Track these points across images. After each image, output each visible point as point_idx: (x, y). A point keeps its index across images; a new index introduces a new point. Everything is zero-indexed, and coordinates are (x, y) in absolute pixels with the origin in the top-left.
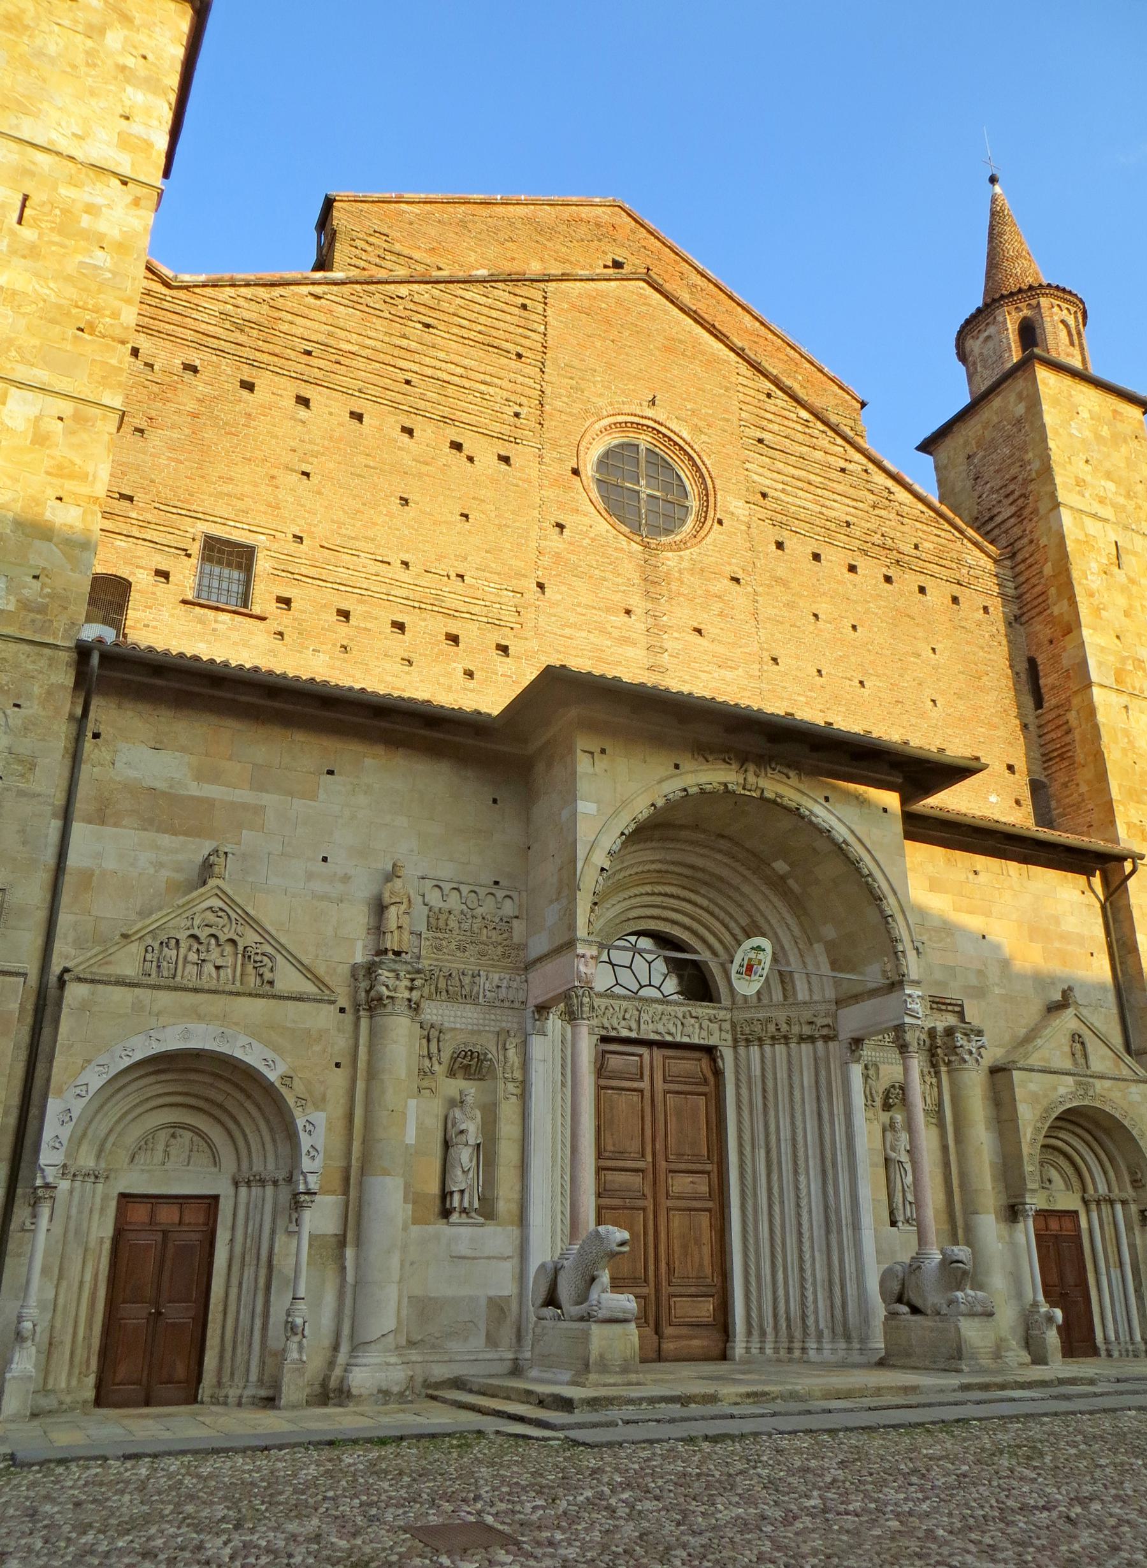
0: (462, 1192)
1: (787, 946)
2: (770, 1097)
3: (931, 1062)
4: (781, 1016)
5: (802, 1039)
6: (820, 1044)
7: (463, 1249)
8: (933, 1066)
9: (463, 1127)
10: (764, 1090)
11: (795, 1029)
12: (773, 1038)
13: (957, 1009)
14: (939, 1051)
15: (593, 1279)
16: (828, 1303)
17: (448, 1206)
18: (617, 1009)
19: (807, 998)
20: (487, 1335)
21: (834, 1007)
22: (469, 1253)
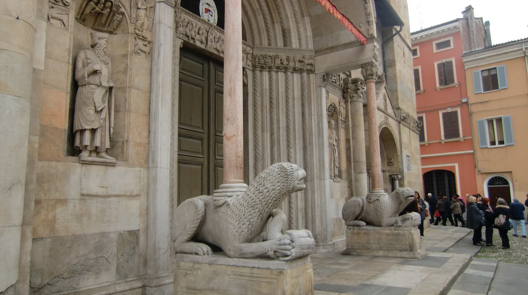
0: (93, 131)
1: (289, 15)
2: (274, 101)
3: (343, 96)
4: (283, 56)
5: (295, 70)
6: (305, 74)
7: (95, 189)
8: (344, 98)
9: (97, 67)
10: (271, 98)
11: (292, 64)
12: (278, 68)
13: (348, 73)
14: (349, 90)
15: (271, 215)
16: (304, 220)
17: (77, 143)
18: (194, 25)
19: (298, 47)
20: (117, 269)
21: (314, 55)
22: (101, 191)
